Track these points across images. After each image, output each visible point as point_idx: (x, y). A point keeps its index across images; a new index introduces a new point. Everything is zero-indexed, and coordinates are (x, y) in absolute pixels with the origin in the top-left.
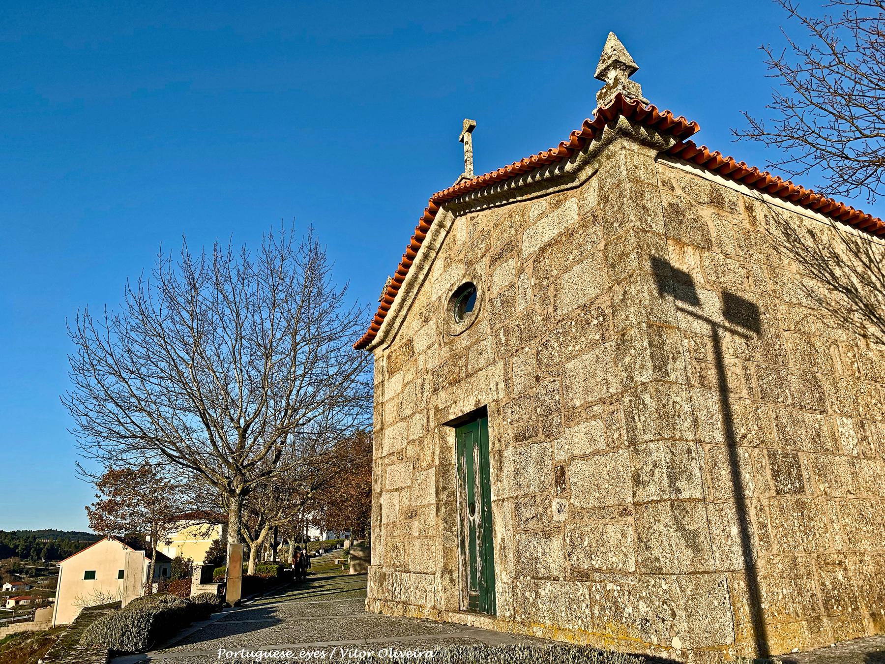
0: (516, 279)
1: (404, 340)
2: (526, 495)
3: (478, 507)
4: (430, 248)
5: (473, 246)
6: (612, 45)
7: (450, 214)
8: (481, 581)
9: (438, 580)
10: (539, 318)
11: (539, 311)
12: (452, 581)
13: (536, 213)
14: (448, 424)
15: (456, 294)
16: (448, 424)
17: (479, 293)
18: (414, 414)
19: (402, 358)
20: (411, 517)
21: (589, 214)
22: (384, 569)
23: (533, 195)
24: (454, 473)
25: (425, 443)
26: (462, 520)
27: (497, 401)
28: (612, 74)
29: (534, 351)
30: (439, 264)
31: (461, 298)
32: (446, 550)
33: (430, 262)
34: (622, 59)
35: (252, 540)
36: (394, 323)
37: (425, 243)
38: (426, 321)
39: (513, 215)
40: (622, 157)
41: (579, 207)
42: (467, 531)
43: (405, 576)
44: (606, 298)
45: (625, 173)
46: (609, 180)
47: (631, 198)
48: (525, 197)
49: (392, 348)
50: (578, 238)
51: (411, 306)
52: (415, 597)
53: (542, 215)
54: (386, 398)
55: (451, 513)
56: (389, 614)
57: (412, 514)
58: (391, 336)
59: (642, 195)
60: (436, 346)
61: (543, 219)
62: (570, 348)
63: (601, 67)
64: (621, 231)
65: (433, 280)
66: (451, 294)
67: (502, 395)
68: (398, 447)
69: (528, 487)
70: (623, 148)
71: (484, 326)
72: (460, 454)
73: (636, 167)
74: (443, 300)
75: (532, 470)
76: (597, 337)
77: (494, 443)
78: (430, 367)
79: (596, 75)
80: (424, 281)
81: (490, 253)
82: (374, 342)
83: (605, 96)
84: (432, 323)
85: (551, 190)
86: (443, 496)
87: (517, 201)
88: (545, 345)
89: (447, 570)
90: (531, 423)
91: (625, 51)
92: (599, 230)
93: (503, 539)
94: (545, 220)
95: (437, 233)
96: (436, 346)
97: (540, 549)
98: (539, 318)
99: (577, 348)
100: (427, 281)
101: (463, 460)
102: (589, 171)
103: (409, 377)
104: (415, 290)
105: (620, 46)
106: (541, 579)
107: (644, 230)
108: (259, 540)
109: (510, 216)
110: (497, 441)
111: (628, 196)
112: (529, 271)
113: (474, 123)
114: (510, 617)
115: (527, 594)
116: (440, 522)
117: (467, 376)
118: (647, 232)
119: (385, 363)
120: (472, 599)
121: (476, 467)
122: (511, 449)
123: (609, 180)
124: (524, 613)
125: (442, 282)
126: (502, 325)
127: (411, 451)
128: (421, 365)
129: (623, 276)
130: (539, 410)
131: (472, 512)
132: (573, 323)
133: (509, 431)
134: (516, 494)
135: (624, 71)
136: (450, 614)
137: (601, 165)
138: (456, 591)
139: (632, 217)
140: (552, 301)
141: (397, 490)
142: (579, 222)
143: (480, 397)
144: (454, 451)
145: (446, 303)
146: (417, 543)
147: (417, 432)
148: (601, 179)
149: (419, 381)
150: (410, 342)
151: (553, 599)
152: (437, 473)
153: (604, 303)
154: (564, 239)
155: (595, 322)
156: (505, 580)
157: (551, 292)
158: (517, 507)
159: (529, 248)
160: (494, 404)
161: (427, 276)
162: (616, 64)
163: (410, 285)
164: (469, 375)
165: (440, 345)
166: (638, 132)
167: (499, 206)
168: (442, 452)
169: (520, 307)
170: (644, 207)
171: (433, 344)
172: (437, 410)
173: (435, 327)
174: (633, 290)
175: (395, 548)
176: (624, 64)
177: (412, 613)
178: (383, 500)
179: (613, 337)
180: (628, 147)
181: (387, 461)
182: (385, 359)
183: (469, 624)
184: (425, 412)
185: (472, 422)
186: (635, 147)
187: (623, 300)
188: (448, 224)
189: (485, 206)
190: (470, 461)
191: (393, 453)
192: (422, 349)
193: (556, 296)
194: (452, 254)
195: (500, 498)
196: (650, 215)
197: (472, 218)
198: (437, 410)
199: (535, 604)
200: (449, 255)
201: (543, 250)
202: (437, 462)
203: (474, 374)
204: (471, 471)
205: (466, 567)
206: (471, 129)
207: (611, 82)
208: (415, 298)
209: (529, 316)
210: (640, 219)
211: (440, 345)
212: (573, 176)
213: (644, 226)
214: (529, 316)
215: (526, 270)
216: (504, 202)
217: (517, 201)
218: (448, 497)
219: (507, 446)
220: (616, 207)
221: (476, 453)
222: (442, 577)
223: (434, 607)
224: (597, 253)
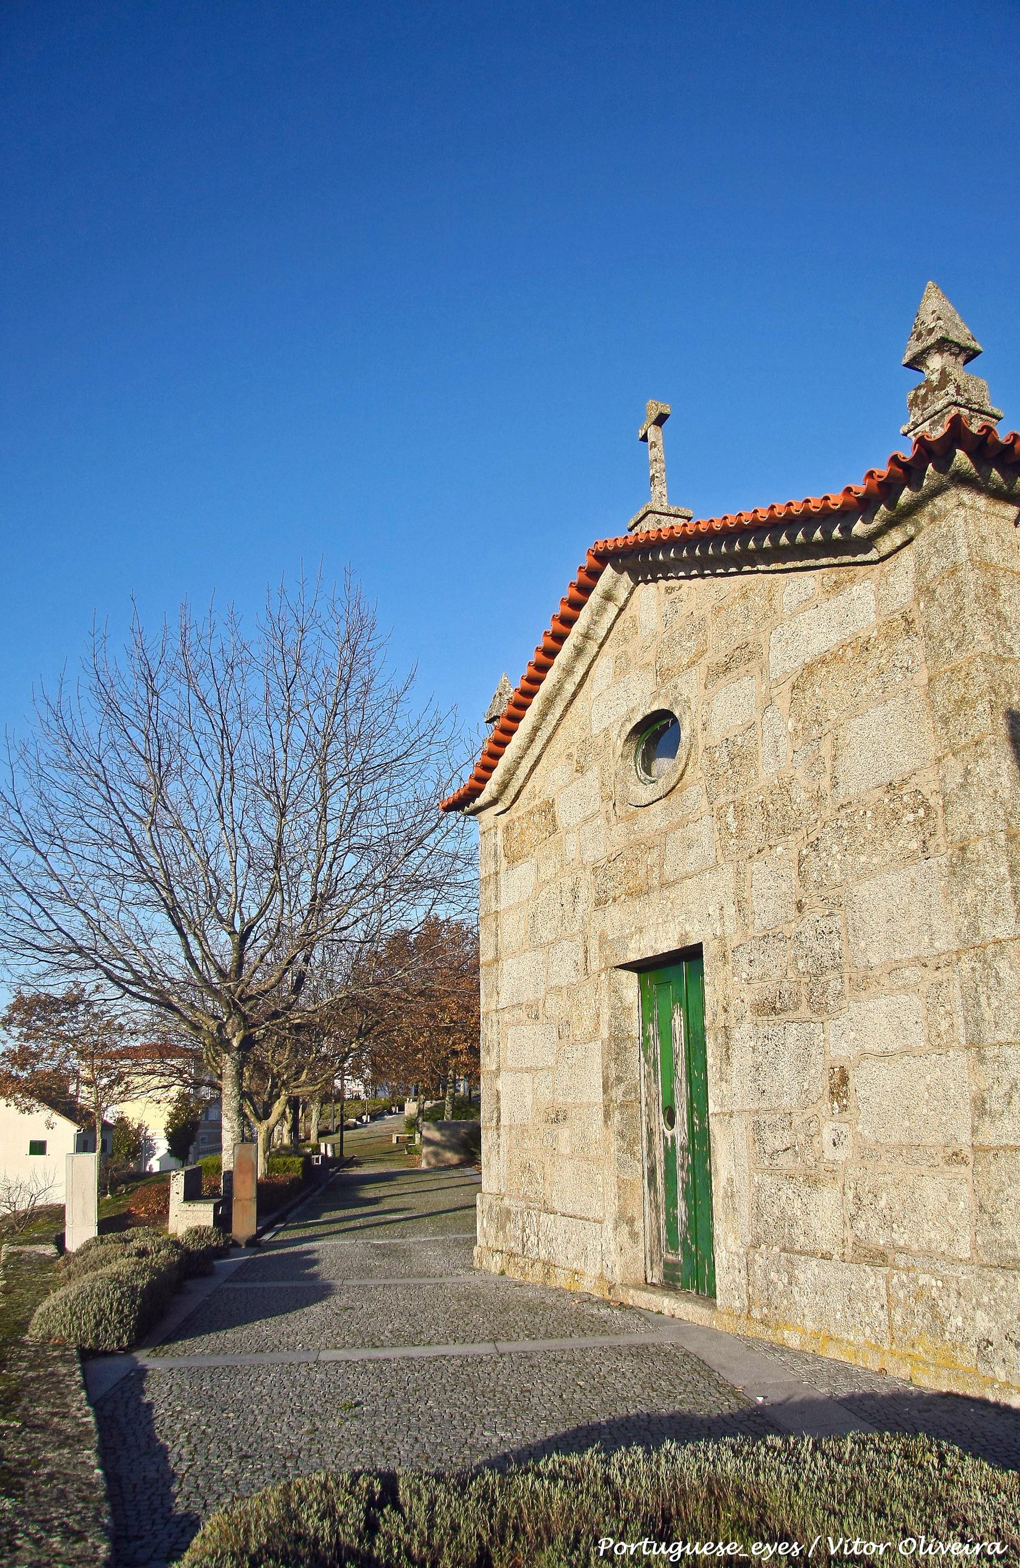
0: (757, 717)
1: (537, 802)
2: (774, 1110)
3: (681, 1115)
4: (586, 637)
5: (671, 642)
6: (934, 308)
7: (626, 576)
8: (685, 1239)
9: (609, 1232)
10: (804, 796)
11: (804, 782)
12: (634, 1235)
13: (795, 598)
14: (625, 967)
15: (639, 729)
16: (625, 967)
17: (684, 734)
18: (558, 940)
19: (532, 835)
20: (556, 1121)
21: (897, 616)
22: (507, 1202)
23: (789, 565)
24: (635, 1054)
25: (581, 995)
26: (651, 1133)
27: (722, 939)
28: (935, 362)
29: (794, 855)
30: (604, 666)
31: (646, 736)
32: (622, 1185)
33: (586, 660)
34: (952, 337)
35: (260, 1119)
36: (516, 768)
37: (578, 628)
38: (580, 770)
39: (751, 594)
40: (960, 521)
41: (879, 600)
42: (659, 1153)
43: (544, 1216)
44: (931, 776)
45: (964, 551)
46: (934, 559)
47: (977, 598)
48: (773, 567)
49: (513, 814)
50: (877, 658)
51: (549, 740)
52: (566, 1256)
53: (807, 603)
54: (502, 906)
55: (629, 1123)
56: (518, 1277)
57: (558, 1117)
58: (511, 792)
59: (995, 592)
60: (600, 821)
61: (805, 609)
62: (863, 859)
63: (914, 347)
64: (959, 658)
65: (593, 695)
66: (629, 727)
67: (730, 927)
68: (528, 996)
69: (778, 1097)
70: (961, 504)
71: (694, 792)
72: (646, 1020)
73: (984, 539)
74: (614, 735)
75: (786, 1070)
76: (914, 845)
77: (715, 1014)
78: (589, 857)
79: (905, 361)
80: (574, 695)
81: (704, 661)
82: (479, 801)
83: (924, 402)
84: (592, 775)
85: (824, 561)
86: (617, 1093)
87: (758, 572)
88: (814, 846)
89: (625, 1219)
90: (786, 985)
91: (957, 319)
92: (918, 648)
93: (730, 1181)
94: (812, 613)
95: (601, 611)
96: (600, 821)
97: (797, 1204)
98: (804, 796)
99: (875, 861)
100: (580, 696)
101: (651, 1030)
102: (896, 537)
103: (548, 871)
104: (558, 711)
105: (947, 308)
106: (800, 1253)
107: (999, 658)
108: (272, 1119)
109: (745, 596)
110: (720, 1011)
111: (972, 596)
112: (783, 702)
113: (667, 411)
114: (742, 1310)
115: (773, 1276)
116: (612, 1137)
117: (662, 885)
118: (1005, 661)
119: (499, 839)
120: (670, 1269)
121: (677, 1045)
122: (746, 1027)
123: (934, 559)
124: (768, 1306)
125: (610, 700)
126: (731, 798)
127: (554, 1007)
128: (571, 850)
129: (963, 741)
130: (801, 964)
131: (671, 1121)
132: (869, 814)
133: (743, 995)
134: (754, 1106)
135: (957, 355)
136: (632, 1292)
137: (919, 530)
138: (640, 1250)
139: (980, 636)
140: (828, 765)
141: (528, 1070)
142: (879, 628)
143: (688, 928)
144: (636, 1014)
145: (620, 743)
146: (568, 1168)
147: (565, 973)
148: (919, 555)
149: (569, 882)
150: (549, 806)
151: (822, 1289)
152: (606, 1052)
153: (927, 782)
154: (850, 654)
155: (911, 817)
156: (734, 1249)
157: (826, 749)
158: (757, 1127)
159: (782, 659)
160: (716, 942)
161: (580, 685)
162: (943, 345)
163: (550, 701)
164: (665, 885)
165: (608, 820)
166: (987, 478)
167: (722, 575)
168: (614, 1016)
169: (766, 772)
170: (999, 615)
171: (594, 815)
172: (603, 940)
173: (597, 784)
174: (982, 769)
175: (526, 1168)
176: (957, 345)
177: (561, 1280)
178: (502, 1084)
179: (943, 849)
180: (968, 503)
181: (507, 1017)
182: (500, 832)
183: (666, 1312)
184: (579, 939)
185: (673, 971)
186: (981, 502)
187: (963, 786)
188: (622, 594)
189: (694, 572)
190: (666, 1034)
191: (519, 1005)
192: (573, 822)
193: (835, 758)
194: (630, 650)
195: (725, 1110)
196: (1009, 629)
197: (669, 590)
198: (603, 940)
199: (787, 1294)
200: (625, 652)
201: (809, 669)
202: (605, 1033)
203: (675, 882)
204: (668, 1050)
205: (658, 1212)
206: (661, 420)
207: (935, 377)
208: (558, 725)
209: (784, 788)
210: (993, 638)
211: (608, 820)
212: (867, 543)
213: (1000, 651)
214: (784, 788)
215: (778, 701)
216: (733, 570)
217: (758, 572)
218: (625, 1093)
219: (740, 1020)
220: (949, 614)
221: (678, 1022)
222: (615, 1229)
223: (601, 1277)
224: (915, 691)
